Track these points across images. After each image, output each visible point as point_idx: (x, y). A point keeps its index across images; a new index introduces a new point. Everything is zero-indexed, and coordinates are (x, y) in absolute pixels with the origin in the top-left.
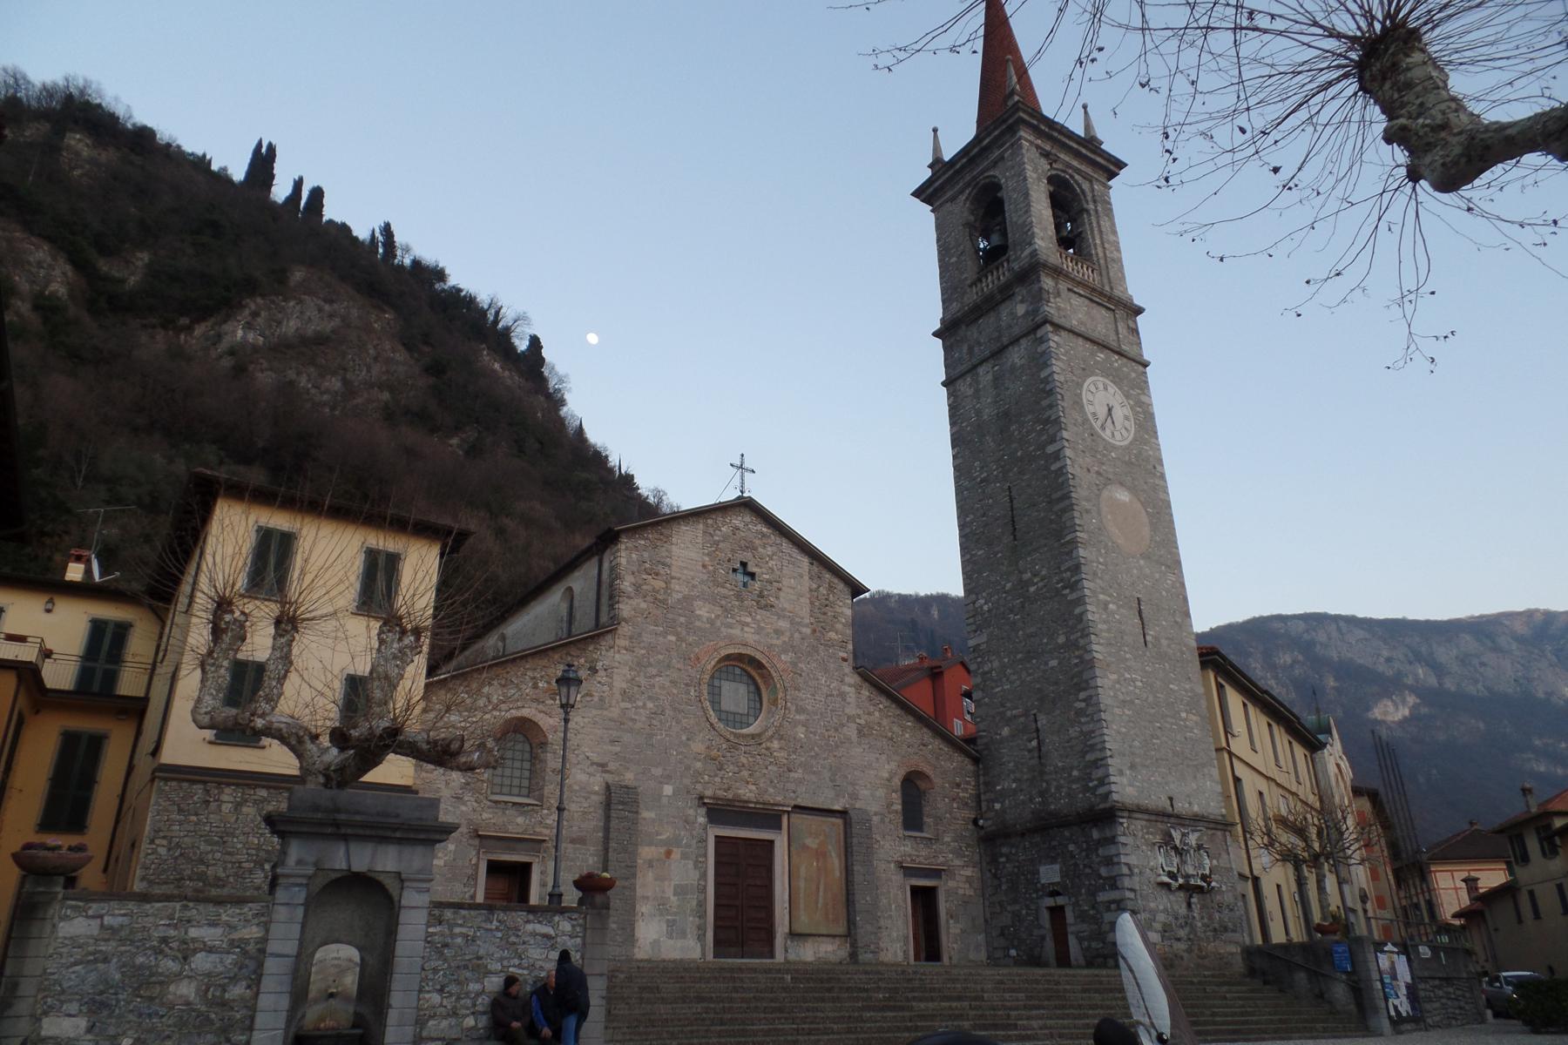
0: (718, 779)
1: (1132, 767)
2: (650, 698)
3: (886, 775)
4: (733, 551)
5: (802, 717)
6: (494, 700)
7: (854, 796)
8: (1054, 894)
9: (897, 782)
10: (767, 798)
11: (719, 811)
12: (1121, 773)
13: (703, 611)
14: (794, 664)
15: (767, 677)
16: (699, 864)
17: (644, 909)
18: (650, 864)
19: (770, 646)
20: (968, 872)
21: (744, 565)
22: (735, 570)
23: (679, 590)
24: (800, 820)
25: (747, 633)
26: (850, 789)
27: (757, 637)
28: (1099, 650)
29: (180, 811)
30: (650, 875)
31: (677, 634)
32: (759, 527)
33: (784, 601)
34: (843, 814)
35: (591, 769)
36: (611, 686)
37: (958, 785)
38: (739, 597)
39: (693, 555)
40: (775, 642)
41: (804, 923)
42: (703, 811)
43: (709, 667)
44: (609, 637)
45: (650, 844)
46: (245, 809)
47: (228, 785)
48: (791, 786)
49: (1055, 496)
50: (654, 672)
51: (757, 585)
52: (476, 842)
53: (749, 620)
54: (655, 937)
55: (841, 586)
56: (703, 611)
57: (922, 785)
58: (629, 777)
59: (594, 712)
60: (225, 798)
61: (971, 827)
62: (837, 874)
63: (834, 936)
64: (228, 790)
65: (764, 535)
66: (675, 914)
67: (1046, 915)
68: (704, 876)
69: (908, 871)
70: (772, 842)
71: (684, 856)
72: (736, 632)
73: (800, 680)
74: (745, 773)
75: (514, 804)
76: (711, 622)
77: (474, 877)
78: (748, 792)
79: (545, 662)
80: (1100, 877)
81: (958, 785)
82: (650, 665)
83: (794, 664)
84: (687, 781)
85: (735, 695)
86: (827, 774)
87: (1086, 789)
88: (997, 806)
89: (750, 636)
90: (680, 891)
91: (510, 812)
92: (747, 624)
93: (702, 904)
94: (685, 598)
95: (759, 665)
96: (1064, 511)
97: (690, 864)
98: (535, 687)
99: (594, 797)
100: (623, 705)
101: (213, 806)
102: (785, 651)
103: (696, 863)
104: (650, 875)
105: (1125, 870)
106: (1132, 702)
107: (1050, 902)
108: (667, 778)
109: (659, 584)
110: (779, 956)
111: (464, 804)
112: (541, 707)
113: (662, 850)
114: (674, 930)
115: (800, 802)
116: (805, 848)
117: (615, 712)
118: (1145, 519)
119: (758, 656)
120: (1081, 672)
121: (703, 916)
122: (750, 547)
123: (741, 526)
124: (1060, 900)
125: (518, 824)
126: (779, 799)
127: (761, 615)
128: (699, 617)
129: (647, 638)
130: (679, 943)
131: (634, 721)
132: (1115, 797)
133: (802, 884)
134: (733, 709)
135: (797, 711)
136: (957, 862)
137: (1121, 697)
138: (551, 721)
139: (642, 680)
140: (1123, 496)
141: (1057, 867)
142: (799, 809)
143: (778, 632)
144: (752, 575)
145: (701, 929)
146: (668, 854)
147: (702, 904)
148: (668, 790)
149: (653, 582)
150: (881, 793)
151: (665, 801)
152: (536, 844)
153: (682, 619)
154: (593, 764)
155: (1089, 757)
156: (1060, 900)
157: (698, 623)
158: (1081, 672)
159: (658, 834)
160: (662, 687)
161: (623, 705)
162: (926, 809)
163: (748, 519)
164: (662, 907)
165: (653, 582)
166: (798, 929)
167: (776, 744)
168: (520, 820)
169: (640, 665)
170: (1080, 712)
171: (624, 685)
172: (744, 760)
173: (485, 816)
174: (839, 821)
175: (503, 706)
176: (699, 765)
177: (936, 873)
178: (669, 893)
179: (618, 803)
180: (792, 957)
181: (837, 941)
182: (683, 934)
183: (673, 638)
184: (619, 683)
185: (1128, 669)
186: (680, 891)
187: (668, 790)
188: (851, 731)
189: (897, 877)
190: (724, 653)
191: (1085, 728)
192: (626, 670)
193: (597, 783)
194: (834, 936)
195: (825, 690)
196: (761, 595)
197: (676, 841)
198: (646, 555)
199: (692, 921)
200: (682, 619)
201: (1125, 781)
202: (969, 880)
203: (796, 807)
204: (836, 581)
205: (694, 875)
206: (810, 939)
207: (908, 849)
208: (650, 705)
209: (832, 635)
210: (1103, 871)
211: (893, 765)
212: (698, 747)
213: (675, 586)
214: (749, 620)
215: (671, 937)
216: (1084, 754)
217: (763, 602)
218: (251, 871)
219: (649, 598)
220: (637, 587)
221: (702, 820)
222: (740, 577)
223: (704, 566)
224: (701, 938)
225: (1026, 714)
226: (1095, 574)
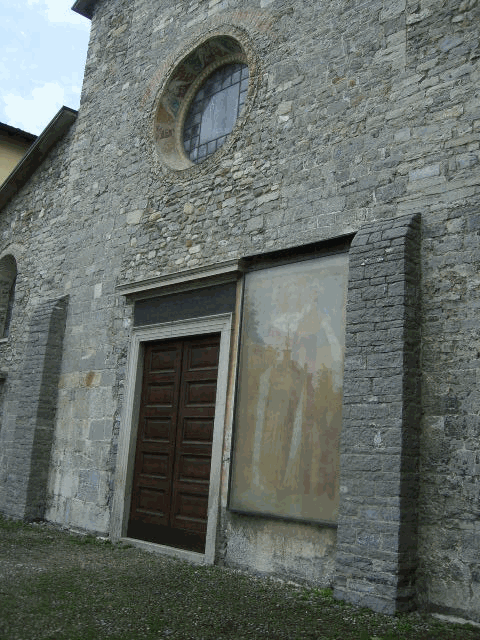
0: (152, 254)
24: (263, 285)
30: (72, 410)
41: (258, 494)
42: (129, 309)
78: (188, 260)
86: (328, 169)
133: (260, 412)
146: (91, 377)
147: (114, 449)
148: (98, 289)
178: (86, 433)
188: (396, 52)
205: (111, 406)
206: (269, 527)
221: (128, 323)
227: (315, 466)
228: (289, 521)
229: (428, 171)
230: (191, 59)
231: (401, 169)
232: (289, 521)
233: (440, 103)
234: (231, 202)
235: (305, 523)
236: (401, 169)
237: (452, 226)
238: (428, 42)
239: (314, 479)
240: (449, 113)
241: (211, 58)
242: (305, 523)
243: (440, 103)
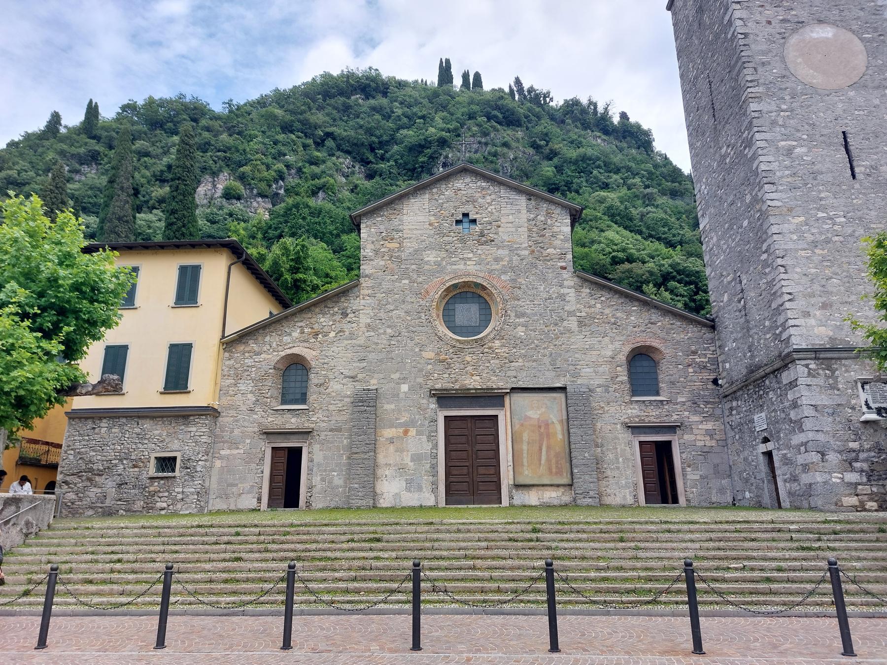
0: (445, 376)
1: (824, 306)
2: (389, 327)
3: (609, 353)
4: (456, 208)
5: (522, 320)
6: (274, 345)
7: (576, 375)
8: (766, 440)
9: (622, 358)
10: (489, 384)
11: (444, 398)
12: (807, 314)
13: (431, 257)
14: (514, 280)
15: (490, 294)
16: (431, 437)
17: (387, 472)
18: (391, 441)
19: (491, 272)
20: (709, 426)
21: (466, 215)
22: (458, 222)
23: (410, 246)
24: (518, 398)
25: (469, 267)
26: (571, 367)
27: (478, 267)
28: (775, 197)
29: (80, 435)
31: (409, 278)
32: (479, 183)
33: (504, 235)
34: (563, 389)
35: (345, 381)
36: (358, 323)
37: (694, 353)
38: (462, 240)
39: (421, 219)
40: (494, 267)
42: (434, 400)
43: (437, 296)
44: (356, 289)
45: (391, 427)
46: (113, 430)
47: (105, 418)
48: (514, 373)
49: (733, 63)
50: (392, 308)
51: (478, 228)
52: (265, 437)
53: (471, 255)
54: (397, 491)
55: (558, 210)
56: (431, 257)
57: (656, 357)
58: (373, 383)
59: (346, 342)
60: (103, 425)
61: (711, 386)
62: (560, 436)
63: (558, 486)
64: (104, 421)
65: (483, 189)
66: (413, 475)
67: (761, 457)
68: (436, 446)
69: (635, 429)
71: (419, 433)
72: (462, 267)
73: (518, 292)
74: (469, 368)
75: (289, 410)
76: (438, 264)
77: (262, 459)
78: (473, 382)
79: (310, 315)
80: (791, 421)
81: (694, 353)
82: (388, 303)
83: (514, 280)
84: (420, 380)
85: (467, 313)
86: (547, 360)
87: (777, 337)
88: (727, 365)
89: (471, 267)
90: (417, 458)
91: (288, 415)
92: (470, 259)
94: (416, 251)
95: (484, 288)
96: (738, 75)
97: (424, 438)
98: (302, 332)
99: (348, 400)
100: (367, 334)
101: (97, 430)
102: (505, 273)
103: (429, 438)
104: (392, 448)
105: (808, 412)
106: (828, 241)
107: (763, 448)
108: (404, 380)
109: (394, 245)
110: (505, 502)
111: (256, 414)
112: (306, 344)
113: (401, 430)
114: (412, 485)
115: (521, 384)
117: (361, 341)
118: (858, 46)
119: (479, 281)
120: (761, 225)
121: (435, 475)
122: (471, 200)
123: (462, 187)
124: (770, 446)
125: (293, 423)
126: (501, 384)
127: (481, 250)
128: (427, 263)
129: (386, 286)
130: (416, 495)
131: (377, 344)
132: (793, 340)
133: (525, 447)
134: (466, 323)
135: (517, 316)
137: (809, 238)
138: (314, 353)
139: (382, 315)
140: (825, 32)
141: (763, 415)
142: (513, 389)
143: (497, 260)
144: (474, 221)
145: (435, 484)
146: (406, 432)
147: (434, 467)
148: (405, 388)
149: (389, 245)
150: (605, 368)
151: (402, 396)
152: (306, 434)
153: (414, 267)
154: (346, 377)
155: (774, 306)
156: (770, 446)
157: (426, 267)
158: (761, 225)
159: (399, 419)
160: (399, 317)
161: (367, 334)
162: (661, 376)
163: (468, 180)
164: (401, 469)
165: (389, 245)
166: (522, 480)
167: (497, 343)
168: (293, 420)
169: (380, 306)
170: (766, 264)
171: (369, 321)
172: (468, 358)
173: (270, 419)
174: (561, 396)
175: (280, 348)
176: (430, 367)
177: (672, 429)
178: (407, 460)
179: (366, 403)
180: (517, 501)
181: (562, 490)
182: (420, 489)
183: (407, 281)
184: (364, 320)
185: (824, 209)
186: (417, 458)
187: (405, 388)
188: (573, 324)
189: (625, 436)
190: (448, 285)
191: (769, 278)
192: (369, 311)
193: (349, 389)
194: (558, 486)
195: (545, 296)
196: (482, 235)
197: (412, 423)
198: (382, 227)
199: (426, 481)
200: (414, 267)
201: (812, 321)
202: (710, 434)
203: (513, 389)
204: (553, 207)
205: (427, 447)
206: (534, 490)
207: (635, 412)
208: (389, 331)
210: (793, 415)
211: (617, 345)
212: (429, 354)
213: (407, 243)
214: (471, 255)
215: (410, 491)
216: (770, 302)
217: (483, 239)
218: (116, 465)
219: (386, 258)
220: (376, 252)
222: (466, 225)
223: (430, 224)
224: (434, 491)
225: (734, 279)
226: (774, 123)
227: (554, 466)
228: (543, 485)
229: (588, 370)
230: (455, 286)
231: (578, 367)
232: (543, 485)
233: (591, 348)
234: (497, 361)
235: (551, 485)
236: (578, 367)
237: (598, 390)
238: (585, 325)
239: (554, 470)
240: (595, 353)
241: (464, 287)
242: (551, 485)
243: (591, 348)
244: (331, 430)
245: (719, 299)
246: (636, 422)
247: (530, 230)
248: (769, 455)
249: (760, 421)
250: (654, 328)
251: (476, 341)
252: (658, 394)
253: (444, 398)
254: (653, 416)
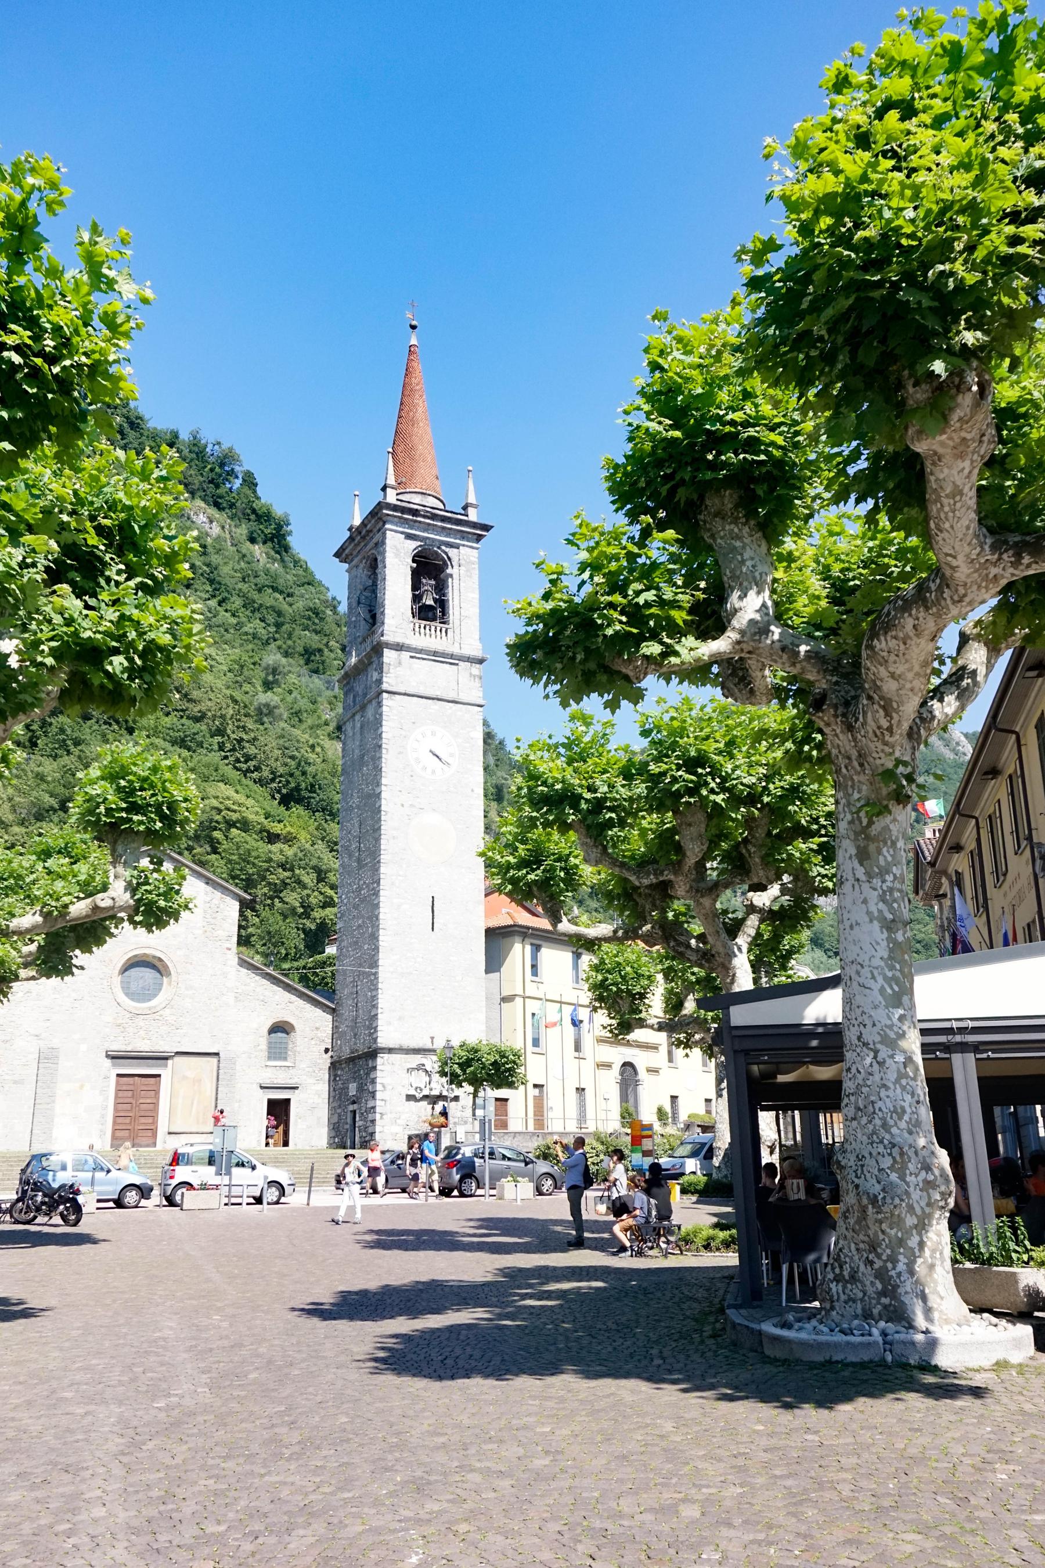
8: (354, 1102)
67: (349, 1116)
70: (159, 1076)
74: (142, 1033)
78: (144, 1046)
93: (103, 1116)
107: (351, 1108)
116: (185, 1078)
124: (355, 1106)
136: (311, 1081)
142: (177, 1053)
146: (82, 1087)
147: (103, 1116)
148: (83, 1047)
167: (167, 1011)
172: (142, 1024)
174: (214, 1060)
187: (83, 1047)
209: (220, 932)
244: (15, 1082)
245: (344, 992)
246: (267, 1082)
247: (205, 912)
248: (354, 1112)
249: (353, 1089)
250: (292, 1007)
251: (150, 1008)
252: (285, 1059)
253: (115, 1057)
254: (281, 1078)
